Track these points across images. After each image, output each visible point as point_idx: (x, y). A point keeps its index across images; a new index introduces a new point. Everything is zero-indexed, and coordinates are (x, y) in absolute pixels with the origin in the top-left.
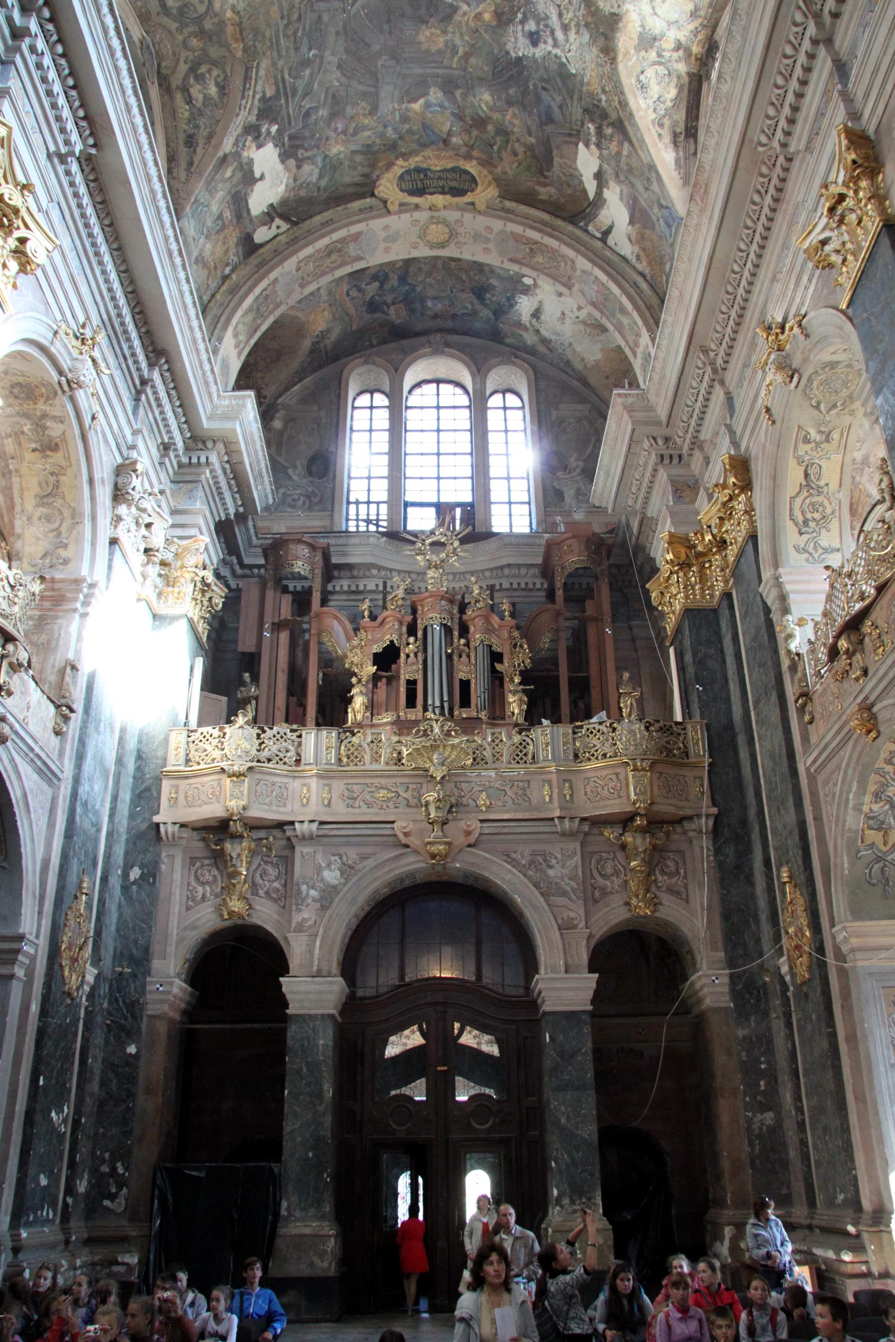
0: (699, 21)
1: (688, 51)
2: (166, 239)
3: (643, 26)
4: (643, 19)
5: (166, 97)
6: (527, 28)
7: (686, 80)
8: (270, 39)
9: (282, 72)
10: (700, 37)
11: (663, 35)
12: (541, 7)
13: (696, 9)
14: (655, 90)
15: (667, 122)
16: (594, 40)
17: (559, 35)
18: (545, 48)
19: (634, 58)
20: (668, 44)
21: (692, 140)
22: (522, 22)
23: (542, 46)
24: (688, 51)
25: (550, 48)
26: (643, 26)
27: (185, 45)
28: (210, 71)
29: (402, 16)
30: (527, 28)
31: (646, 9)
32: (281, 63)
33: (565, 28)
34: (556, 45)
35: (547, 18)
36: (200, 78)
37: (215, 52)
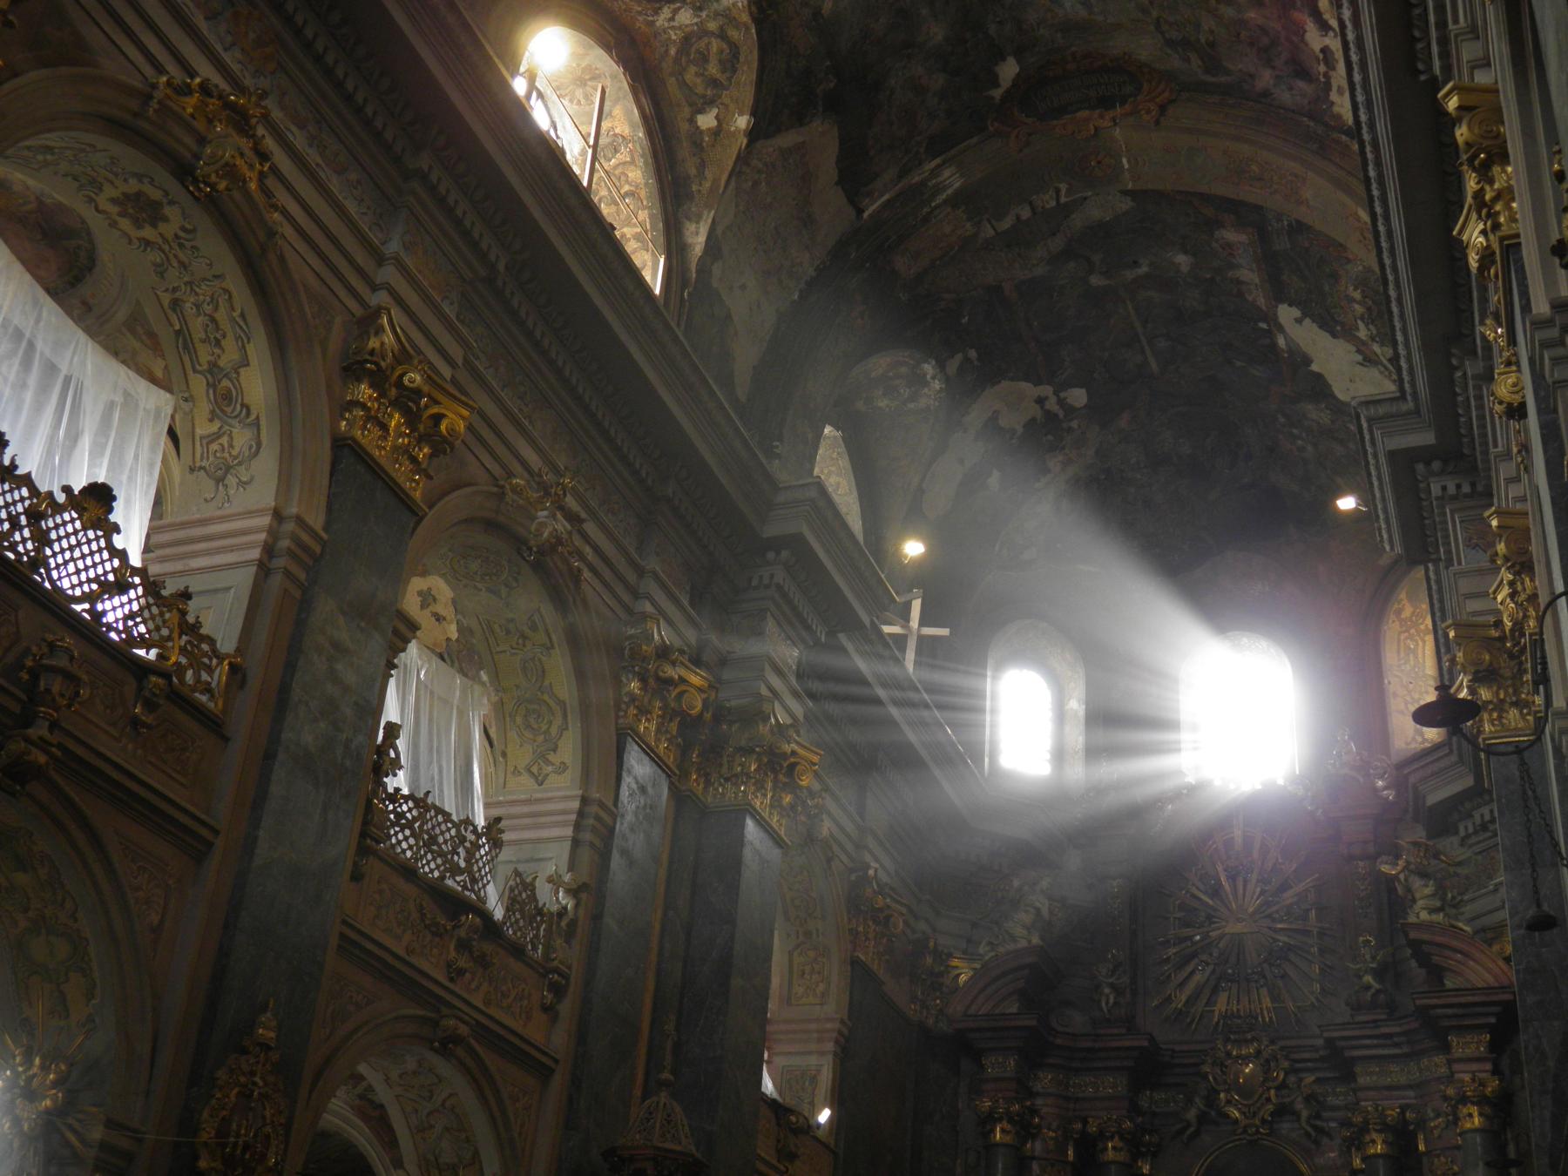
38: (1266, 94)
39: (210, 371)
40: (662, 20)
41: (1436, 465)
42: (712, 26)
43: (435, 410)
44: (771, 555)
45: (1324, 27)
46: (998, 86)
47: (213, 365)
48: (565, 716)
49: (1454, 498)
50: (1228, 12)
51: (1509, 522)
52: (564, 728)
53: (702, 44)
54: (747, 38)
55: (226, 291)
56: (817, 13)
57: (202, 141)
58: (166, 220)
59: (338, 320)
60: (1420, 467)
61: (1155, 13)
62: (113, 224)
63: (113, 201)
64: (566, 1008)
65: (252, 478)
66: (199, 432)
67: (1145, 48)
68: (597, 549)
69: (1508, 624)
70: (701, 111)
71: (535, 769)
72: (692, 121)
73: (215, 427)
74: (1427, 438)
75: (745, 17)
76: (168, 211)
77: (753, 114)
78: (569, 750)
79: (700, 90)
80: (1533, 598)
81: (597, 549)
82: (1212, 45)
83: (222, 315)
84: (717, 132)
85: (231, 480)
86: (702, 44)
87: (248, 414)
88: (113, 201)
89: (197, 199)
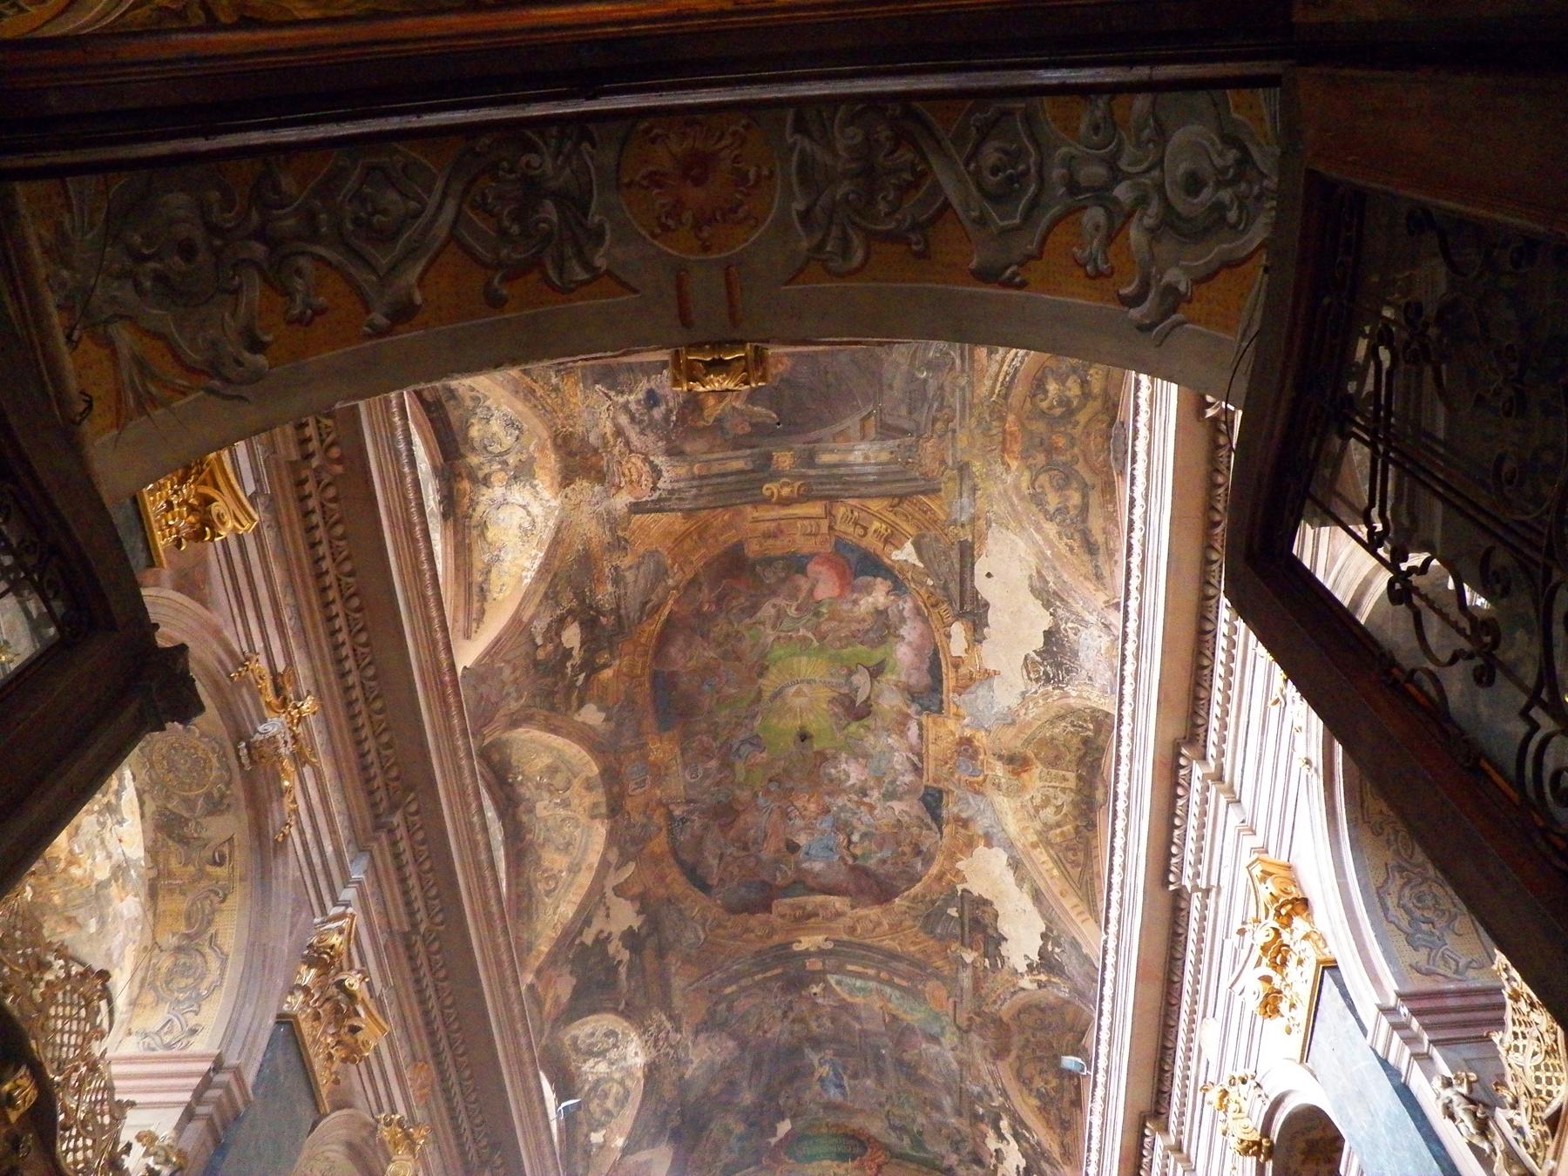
0: (474, 523)
1: (474, 479)
2: (1141, 589)
3: (534, 487)
4: (536, 495)
5: (1112, 393)
6: (663, 408)
7: (463, 450)
8: (971, 416)
9: (963, 371)
10: (466, 500)
11: (508, 486)
12: (651, 437)
13: (482, 535)
14: (496, 426)
15: (469, 403)
16: (584, 440)
17: (624, 420)
18: (633, 398)
19: (532, 448)
20: (498, 478)
21: (429, 399)
22: (670, 411)
23: (641, 396)
24: (474, 479)
25: (632, 398)
26: (534, 487)
27: (1072, 441)
28: (1051, 407)
29: (811, 389)
30: (663, 408)
31: (536, 509)
32: (963, 381)
33: (619, 432)
34: (625, 406)
35: (642, 432)
36: (1064, 402)
37: (1039, 427)
38: (950, 1169)
40: (586, 1067)
42: (617, 1076)
45: (1001, 1137)
46: (774, 1134)
50: (936, 1116)
53: (606, 1086)
54: (637, 1088)
56: (681, 1077)
57: (389, 1160)
61: (887, 1108)
67: (876, 1127)
70: (595, 1131)
72: (587, 1136)
75: (640, 1074)
77: (628, 1138)
79: (597, 1116)
82: (920, 1133)
84: (601, 1147)
86: (606, 1086)
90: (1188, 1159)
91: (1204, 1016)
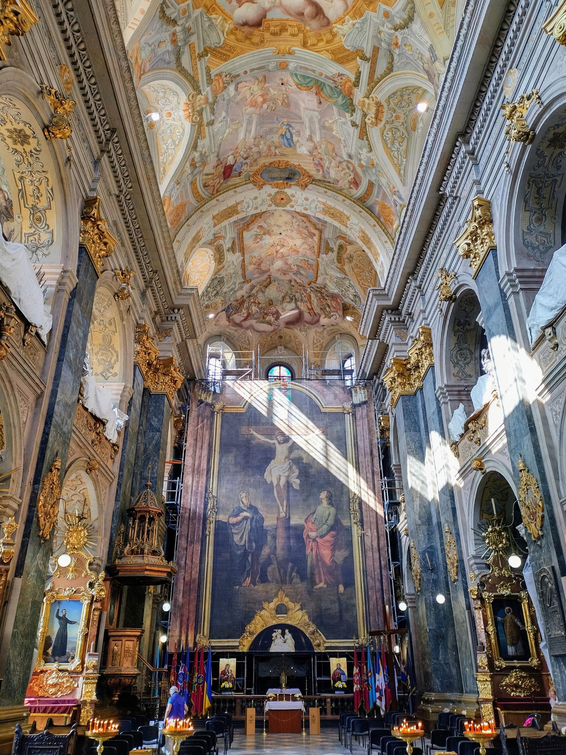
39: (32, 208)
41: (390, 311)
43: (105, 240)
44: (176, 311)
47: (34, 207)
48: (117, 356)
49: (394, 322)
51: (424, 331)
52: (117, 360)
55: (46, 178)
58: (29, 144)
59: (80, 199)
60: (385, 312)
62: (4, 140)
63: (8, 130)
64: (118, 458)
65: (49, 253)
66: (24, 231)
68: (133, 300)
69: (412, 361)
71: (104, 374)
73: (32, 230)
74: (390, 303)
76: (31, 140)
78: (118, 368)
80: (431, 354)
81: (133, 300)
83: (43, 188)
85: (39, 252)
87: (48, 228)
88: (8, 130)
89: (47, 139)
90: (476, 159)
91: (511, 68)
